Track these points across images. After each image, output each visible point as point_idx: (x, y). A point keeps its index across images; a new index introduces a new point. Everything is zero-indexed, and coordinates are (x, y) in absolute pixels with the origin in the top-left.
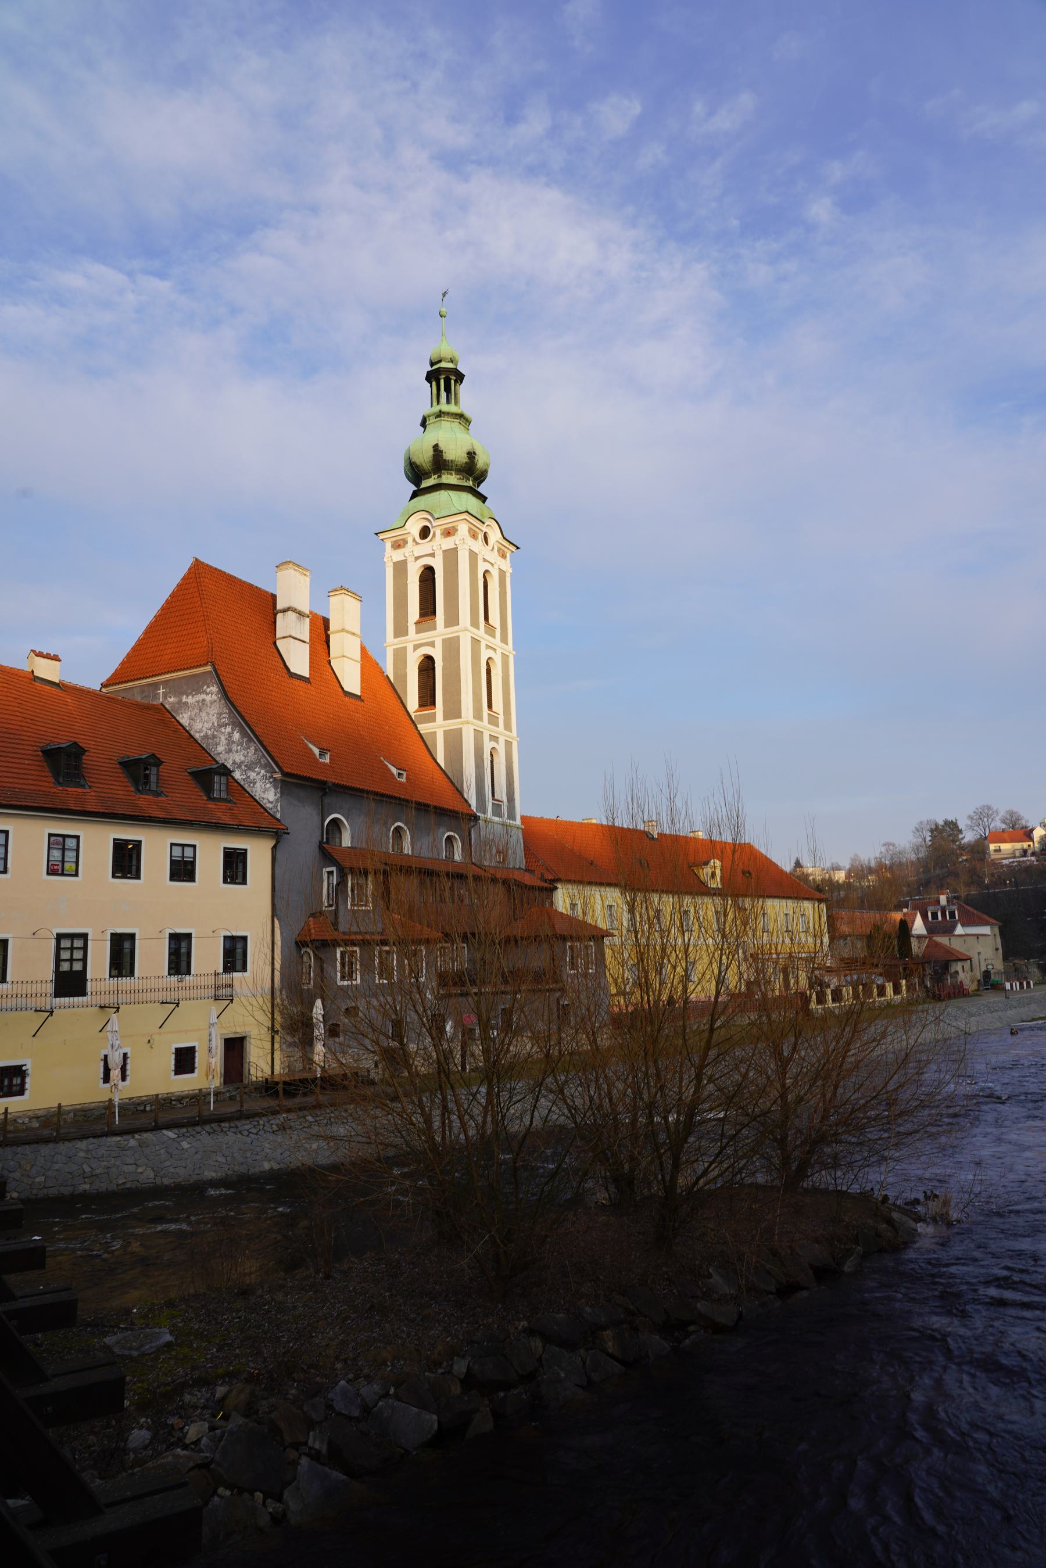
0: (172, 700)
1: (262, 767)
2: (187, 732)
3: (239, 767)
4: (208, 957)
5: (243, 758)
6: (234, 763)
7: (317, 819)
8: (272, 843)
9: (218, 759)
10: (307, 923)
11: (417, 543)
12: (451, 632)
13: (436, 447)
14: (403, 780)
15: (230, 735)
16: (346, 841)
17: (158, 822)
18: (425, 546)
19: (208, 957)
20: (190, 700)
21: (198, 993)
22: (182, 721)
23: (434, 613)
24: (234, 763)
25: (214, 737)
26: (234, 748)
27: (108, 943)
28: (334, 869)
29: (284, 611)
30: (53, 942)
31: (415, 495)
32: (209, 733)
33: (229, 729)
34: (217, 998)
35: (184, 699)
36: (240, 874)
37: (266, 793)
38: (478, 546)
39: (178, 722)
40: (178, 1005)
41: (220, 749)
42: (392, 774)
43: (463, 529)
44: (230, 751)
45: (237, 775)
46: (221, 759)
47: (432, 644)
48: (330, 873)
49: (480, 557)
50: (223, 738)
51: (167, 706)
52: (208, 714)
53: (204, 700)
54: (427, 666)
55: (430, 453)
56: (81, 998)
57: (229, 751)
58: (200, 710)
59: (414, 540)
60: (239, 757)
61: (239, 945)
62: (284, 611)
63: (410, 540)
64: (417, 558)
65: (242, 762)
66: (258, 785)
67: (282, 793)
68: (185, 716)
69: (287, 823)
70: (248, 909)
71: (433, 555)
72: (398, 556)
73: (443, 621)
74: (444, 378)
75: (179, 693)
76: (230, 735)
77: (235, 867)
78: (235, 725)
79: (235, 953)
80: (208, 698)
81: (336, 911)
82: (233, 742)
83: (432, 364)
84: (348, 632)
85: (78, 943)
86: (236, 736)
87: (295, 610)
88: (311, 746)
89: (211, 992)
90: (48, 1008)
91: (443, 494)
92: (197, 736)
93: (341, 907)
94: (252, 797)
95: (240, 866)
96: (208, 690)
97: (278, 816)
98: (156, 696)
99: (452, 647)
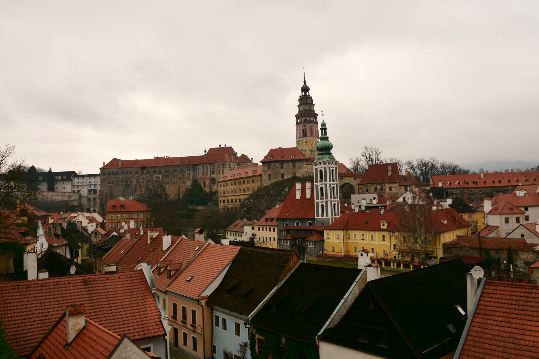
18: (320, 166)
43: (327, 164)
72: (316, 167)
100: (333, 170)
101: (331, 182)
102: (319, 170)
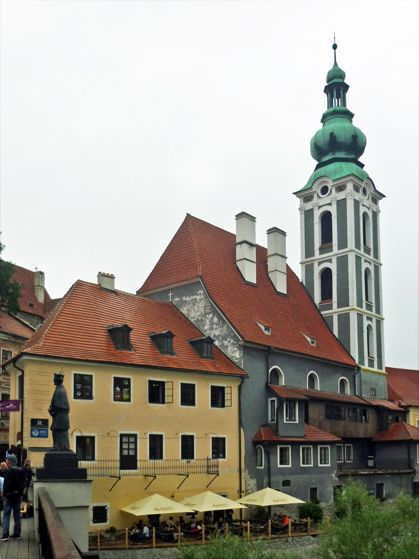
0: (177, 299)
1: (231, 338)
2: (186, 318)
3: (218, 338)
4: (203, 449)
5: (220, 333)
6: (215, 336)
7: (264, 370)
8: (240, 383)
9: (205, 334)
10: (259, 431)
11: (320, 197)
14: (314, 345)
15: (212, 319)
16: (283, 382)
17: (171, 370)
18: (326, 199)
19: (203, 449)
20: (187, 299)
21: (199, 470)
22: (183, 312)
23: (331, 240)
24: (215, 336)
25: (202, 320)
26: (215, 327)
27: (148, 440)
28: (275, 399)
29: (241, 243)
30: (119, 438)
31: (318, 167)
32: (200, 318)
33: (211, 316)
34: (208, 473)
35: (184, 299)
36: (220, 401)
37: (235, 354)
38: (358, 196)
39: (181, 312)
40: (188, 476)
41: (206, 327)
42: (308, 342)
43: (350, 187)
44: (211, 329)
45: (217, 343)
46: (207, 334)
48: (273, 401)
49: (361, 203)
50: (208, 321)
51: (174, 303)
52: (198, 307)
53: (196, 299)
56: (135, 471)
57: (211, 329)
58: (194, 305)
59: (318, 196)
60: (217, 332)
61: (221, 443)
62: (241, 243)
63: (315, 196)
65: (219, 335)
66: (229, 349)
67: (244, 353)
68: (185, 308)
69: (247, 371)
70: (226, 422)
71: (330, 204)
72: (309, 206)
73: (337, 246)
75: (181, 296)
76: (212, 319)
77: (218, 398)
78: (215, 313)
79: (219, 447)
80: (198, 297)
81: (277, 424)
82: (214, 323)
84: (279, 255)
85: (132, 440)
86: (216, 319)
87: (247, 242)
88: (260, 325)
89: (205, 469)
90: (118, 475)
91: (337, 165)
92: (192, 320)
93: (280, 422)
94: (226, 356)
95: (220, 396)
96: (198, 292)
97: (242, 367)
98: (168, 297)
99: (343, 262)
100: (365, 215)
101: (362, 251)
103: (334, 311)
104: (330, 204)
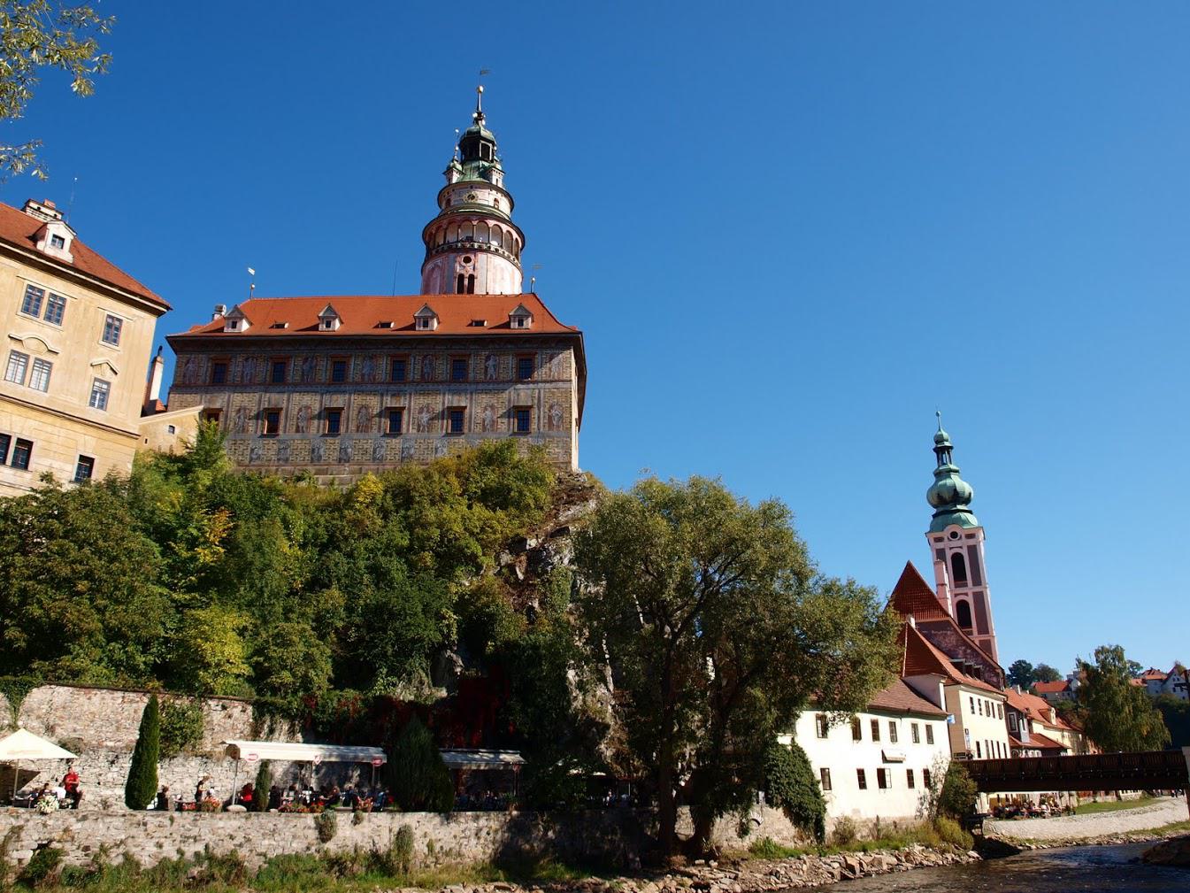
12: (977, 589)
13: (955, 490)
18: (955, 543)
28: (1014, 713)
47: (966, 594)
50: (961, 652)
54: (962, 607)
55: (953, 493)
58: (944, 638)
64: (951, 548)
71: (961, 547)
72: (940, 545)
74: (941, 450)
76: (965, 651)
80: (949, 632)
83: (937, 442)
99: (980, 598)
102: (949, 554)
103: (976, 638)
104: (961, 547)
